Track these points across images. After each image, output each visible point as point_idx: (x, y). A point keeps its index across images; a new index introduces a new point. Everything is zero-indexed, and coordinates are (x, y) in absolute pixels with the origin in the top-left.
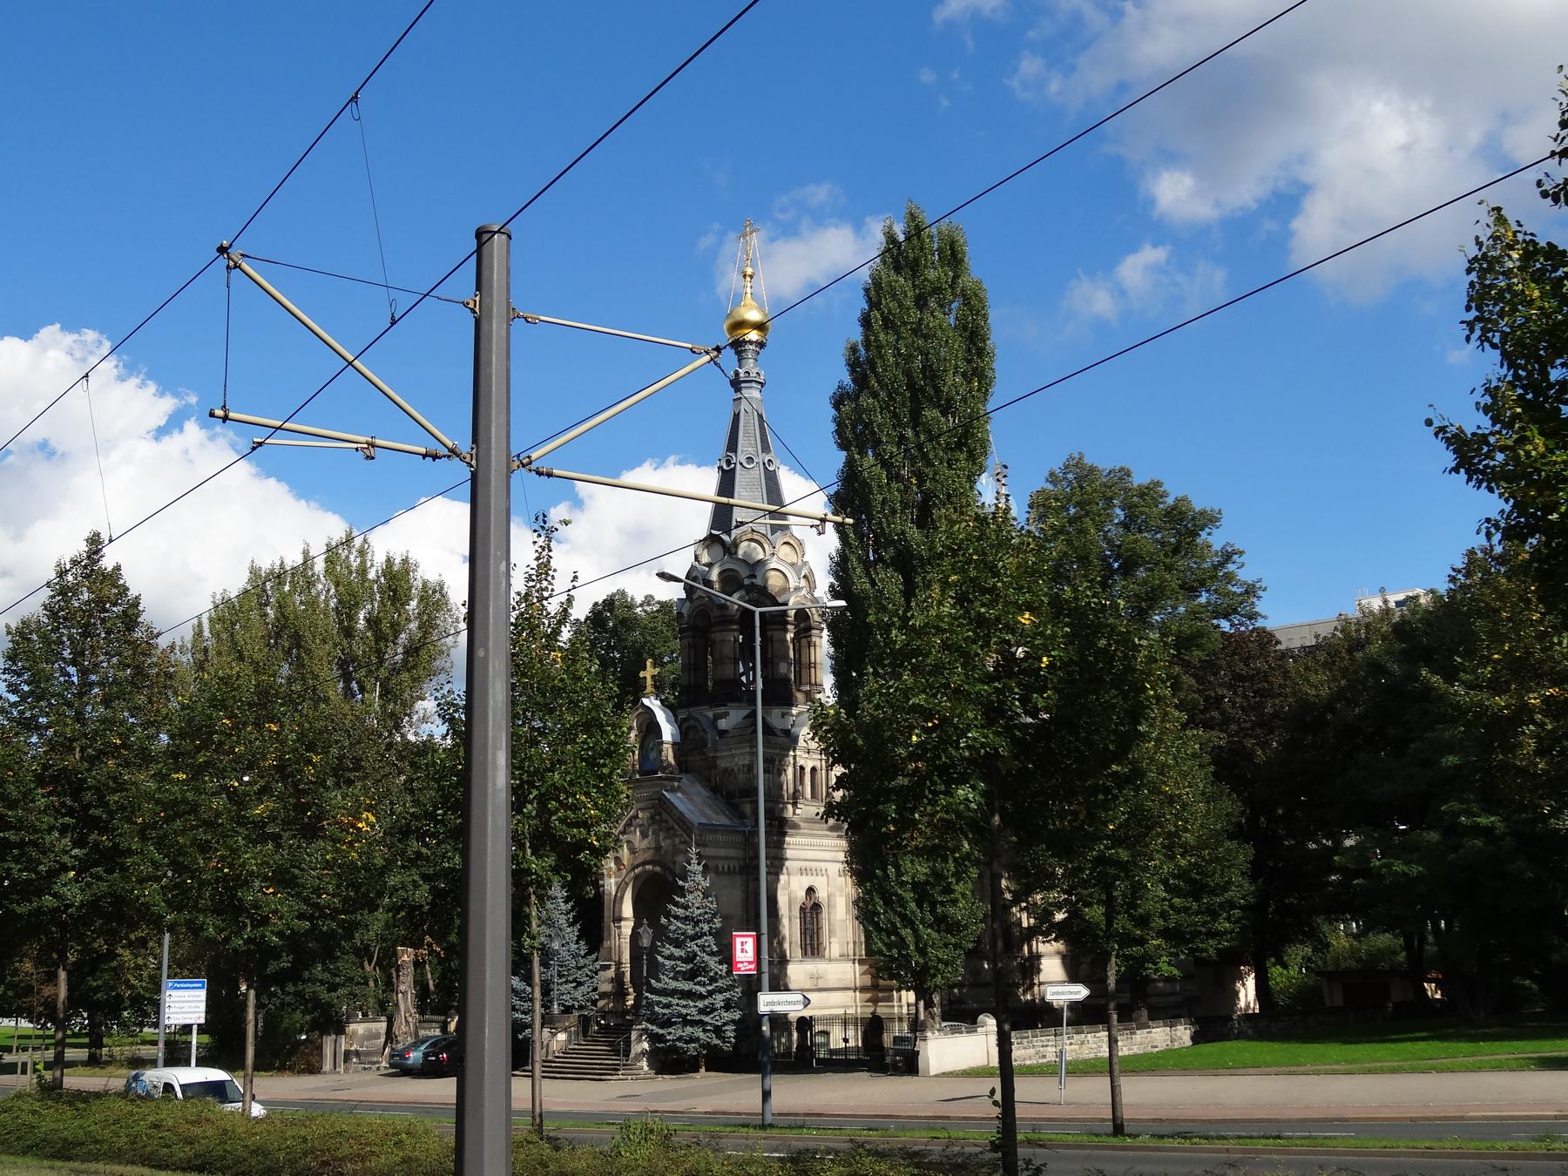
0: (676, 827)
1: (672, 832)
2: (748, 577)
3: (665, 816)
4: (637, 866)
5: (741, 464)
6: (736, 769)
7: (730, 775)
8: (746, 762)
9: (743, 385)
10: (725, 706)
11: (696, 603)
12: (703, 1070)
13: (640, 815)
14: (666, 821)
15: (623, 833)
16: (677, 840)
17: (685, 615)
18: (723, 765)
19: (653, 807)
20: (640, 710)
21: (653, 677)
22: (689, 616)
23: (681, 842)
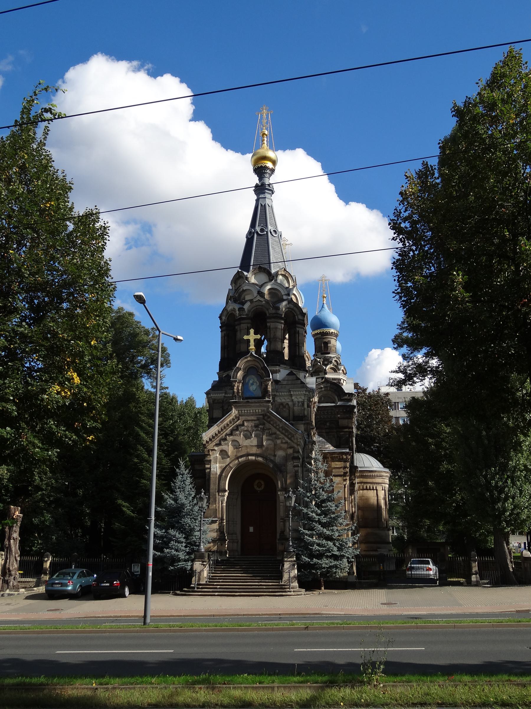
0: (278, 432)
1: (274, 436)
2: (286, 295)
3: (268, 425)
4: (241, 457)
5: (271, 232)
6: (290, 404)
7: (284, 407)
8: (300, 400)
9: (266, 191)
10: (279, 366)
11: (254, 304)
12: (323, 588)
13: (246, 424)
14: (269, 429)
15: (231, 434)
16: (279, 441)
17: (246, 310)
18: (279, 401)
19: (258, 420)
20: (249, 359)
21: (255, 340)
22: (249, 311)
23: (282, 443)
